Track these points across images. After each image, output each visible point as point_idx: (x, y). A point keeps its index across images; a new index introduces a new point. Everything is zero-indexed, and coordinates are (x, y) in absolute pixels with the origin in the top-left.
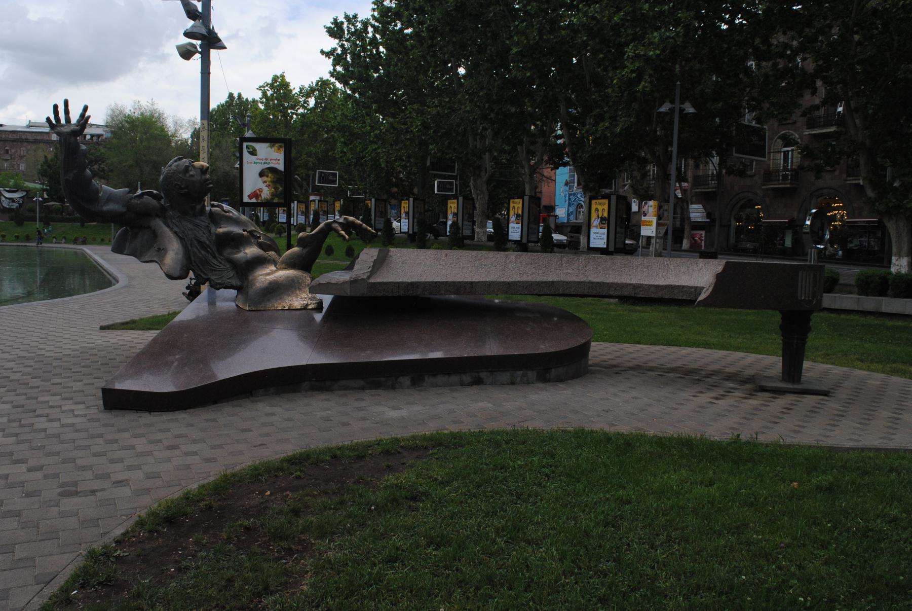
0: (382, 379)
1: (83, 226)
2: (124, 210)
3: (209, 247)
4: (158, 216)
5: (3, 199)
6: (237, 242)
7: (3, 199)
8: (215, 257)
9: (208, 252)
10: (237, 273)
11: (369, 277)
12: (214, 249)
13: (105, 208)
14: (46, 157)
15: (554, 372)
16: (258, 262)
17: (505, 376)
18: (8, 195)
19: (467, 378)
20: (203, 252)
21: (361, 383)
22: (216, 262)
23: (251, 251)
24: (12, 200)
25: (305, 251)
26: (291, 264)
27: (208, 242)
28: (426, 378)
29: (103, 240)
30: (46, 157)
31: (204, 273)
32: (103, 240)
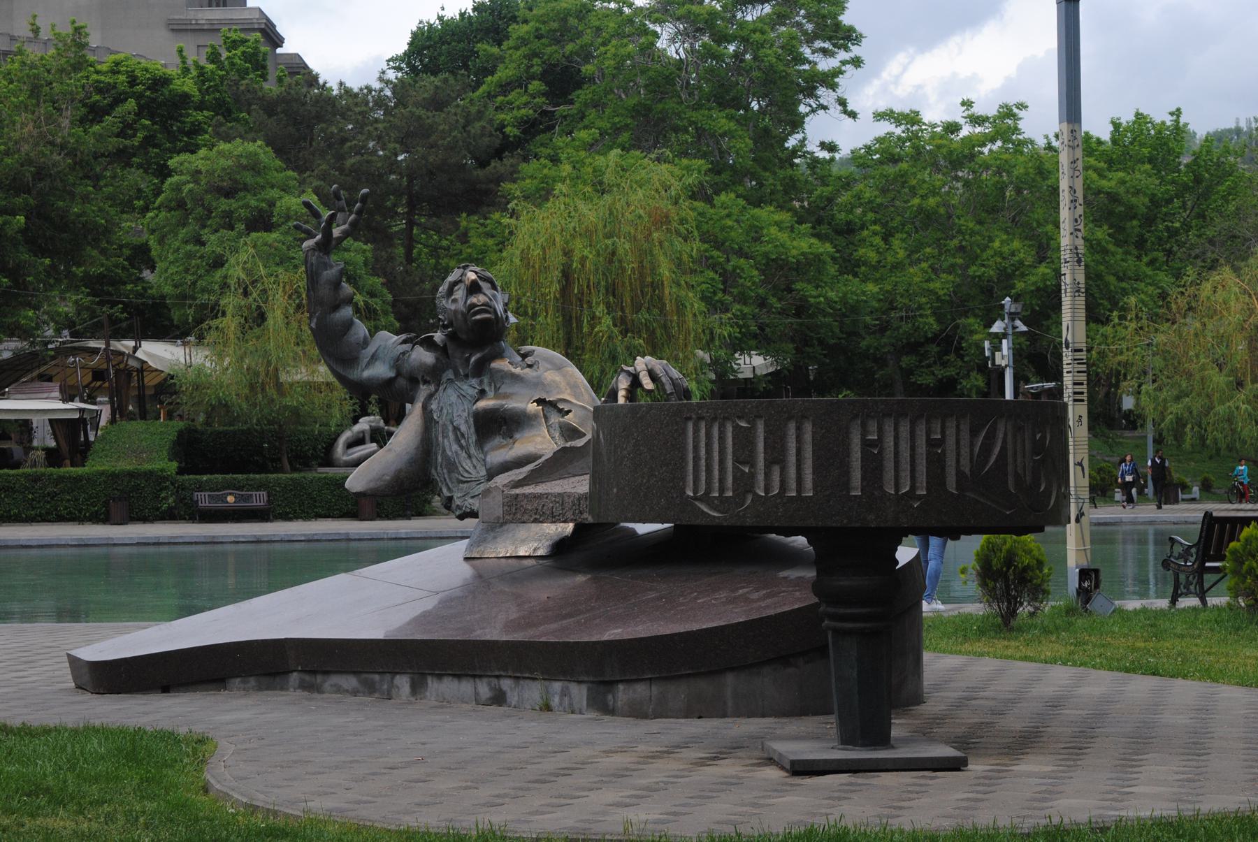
0: (377, 677)
2: (392, 374)
3: (463, 435)
4: (426, 382)
8: (470, 457)
9: (462, 447)
12: (474, 438)
13: (366, 374)
15: (622, 695)
17: (533, 691)
19: (484, 689)
20: (455, 447)
21: (350, 682)
22: (467, 464)
27: (463, 428)
28: (429, 679)
31: (449, 489)
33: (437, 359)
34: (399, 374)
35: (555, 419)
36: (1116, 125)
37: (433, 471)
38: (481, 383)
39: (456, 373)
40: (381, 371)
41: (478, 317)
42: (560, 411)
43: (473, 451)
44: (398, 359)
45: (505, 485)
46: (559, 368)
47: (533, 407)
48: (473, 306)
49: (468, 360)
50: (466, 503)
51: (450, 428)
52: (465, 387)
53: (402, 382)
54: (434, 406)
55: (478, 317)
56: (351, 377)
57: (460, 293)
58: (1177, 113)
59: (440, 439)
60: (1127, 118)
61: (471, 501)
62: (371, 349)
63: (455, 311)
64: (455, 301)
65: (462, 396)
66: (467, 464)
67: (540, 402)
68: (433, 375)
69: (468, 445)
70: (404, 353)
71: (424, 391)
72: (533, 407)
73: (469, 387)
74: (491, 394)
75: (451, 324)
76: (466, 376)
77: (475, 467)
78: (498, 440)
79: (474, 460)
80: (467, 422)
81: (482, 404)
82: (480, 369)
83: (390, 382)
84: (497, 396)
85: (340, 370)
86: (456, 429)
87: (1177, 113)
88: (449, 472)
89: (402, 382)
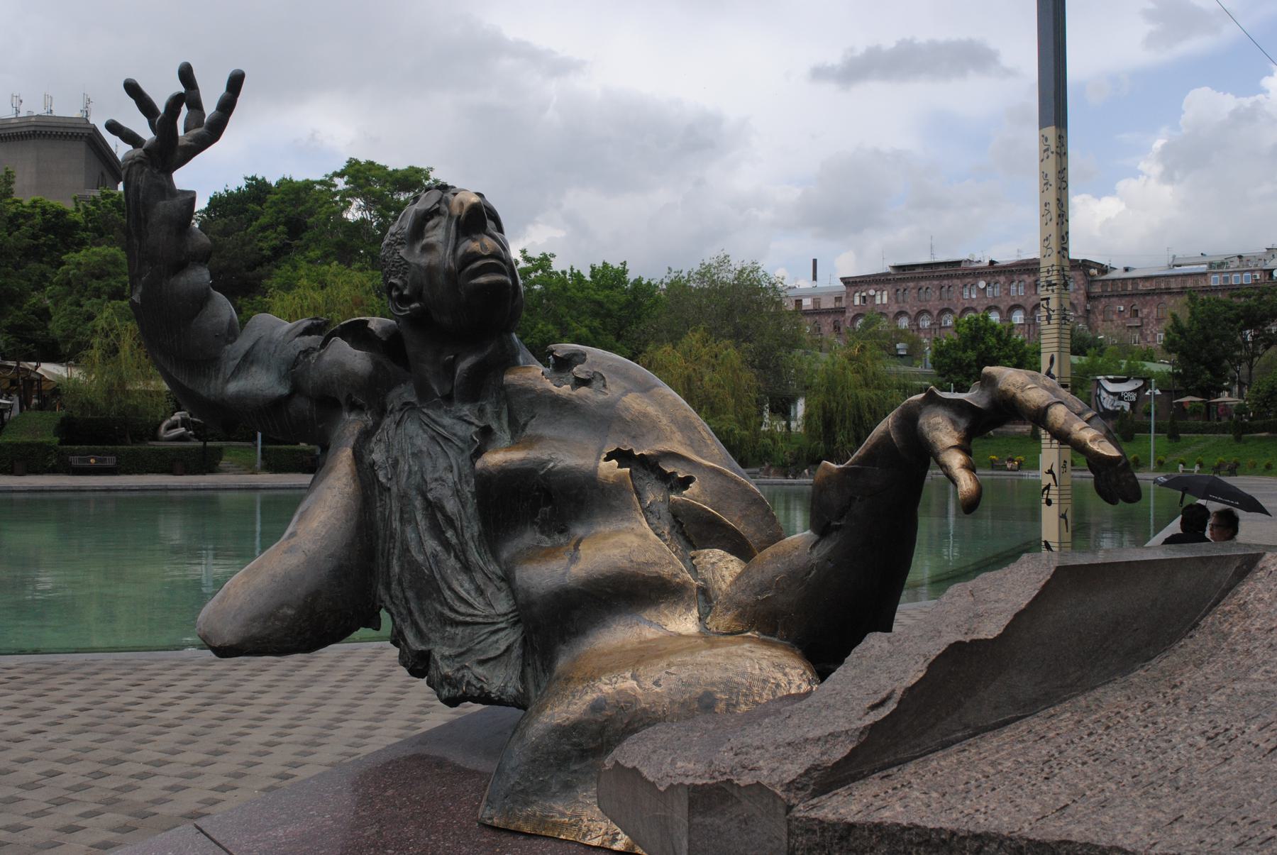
1: (1238, 439)
2: (283, 390)
3: (450, 521)
4: (354, 407)
5: (1104, 394)
6: (554, 503)
7: (1104, 394)
8: (467, 568)
9: (446, 544)
10: (525, 642)
11: (831, 778)
13: (233, 387)
14: (1174, 317)
16: (632, 592)
18: (1112, 387)
20: (431, 544)
22: (462, 585)
23: (624, 542)
24: (1119, 396)
25: (825, 548)
26: (765, 618)
27: (451, 506)
29: (1268, 467)
30: (1174, 317)
31: (421, 635)
32: (1268, 467)
33: (376, 365)
34: (296, 390)
35: (654, 494)
36: (593, 268)
37: (381, 590)
38: (481, 411)
39: (424, 392)
40: (262, 382)
41: (482, 280)
42: (665, 478)
43: (474, 556)
44: (295, 362)
45: (790, 786)
46: (645, 389)
47: (609, 469)
48: (472, 257)
49: (450, 368)
50: (468, 675)
51: (418, 503)
52: (447, 421)
53: (302, 405)
54: (377, 455)
55: (482, 280)
56: (203, 392)
57: (437, 234)
58: (624, 264)
59: (396, 524)
60: (599, 265)
61: (479, 670)
62: (243, 344)
63: (430, 270)
64: (429, 248)
65: (439, 439)
66: (462, 585)
67: (622, 456)
68: (370, 395)
69: (463, 544)
70: (306, 352)
71: (351, 425)
72: (609, 469)
73: (458, 422)
74: (505, 437)
75: (417, 295)
76: (448, 399)
77: (481, 592)
78: (530, 538)
79: (479, 577)
80: (457, 493)
81: (495, 458)
82: (483, 384)
83: (278, 404)
84: (516, 443)
85: (183, 379)
86: (433, 508)
87: (624, 264)
88: (419, 597)
89: (302, 405)
